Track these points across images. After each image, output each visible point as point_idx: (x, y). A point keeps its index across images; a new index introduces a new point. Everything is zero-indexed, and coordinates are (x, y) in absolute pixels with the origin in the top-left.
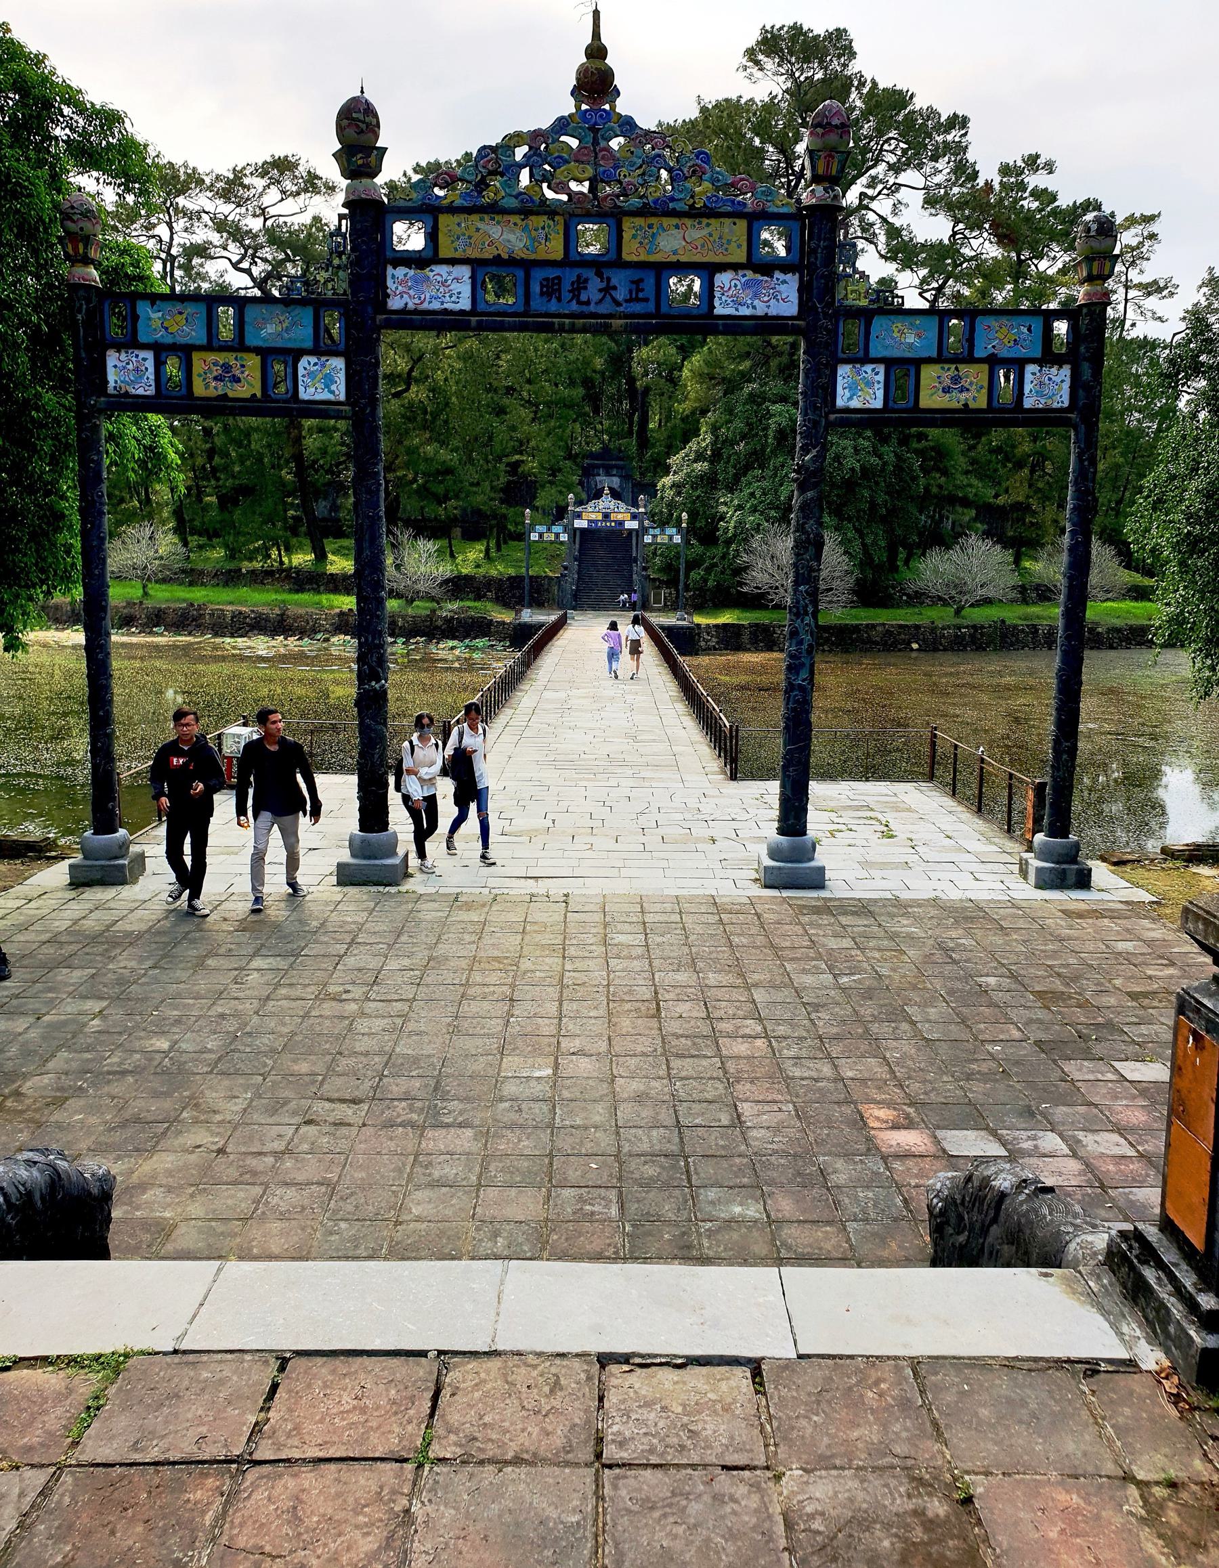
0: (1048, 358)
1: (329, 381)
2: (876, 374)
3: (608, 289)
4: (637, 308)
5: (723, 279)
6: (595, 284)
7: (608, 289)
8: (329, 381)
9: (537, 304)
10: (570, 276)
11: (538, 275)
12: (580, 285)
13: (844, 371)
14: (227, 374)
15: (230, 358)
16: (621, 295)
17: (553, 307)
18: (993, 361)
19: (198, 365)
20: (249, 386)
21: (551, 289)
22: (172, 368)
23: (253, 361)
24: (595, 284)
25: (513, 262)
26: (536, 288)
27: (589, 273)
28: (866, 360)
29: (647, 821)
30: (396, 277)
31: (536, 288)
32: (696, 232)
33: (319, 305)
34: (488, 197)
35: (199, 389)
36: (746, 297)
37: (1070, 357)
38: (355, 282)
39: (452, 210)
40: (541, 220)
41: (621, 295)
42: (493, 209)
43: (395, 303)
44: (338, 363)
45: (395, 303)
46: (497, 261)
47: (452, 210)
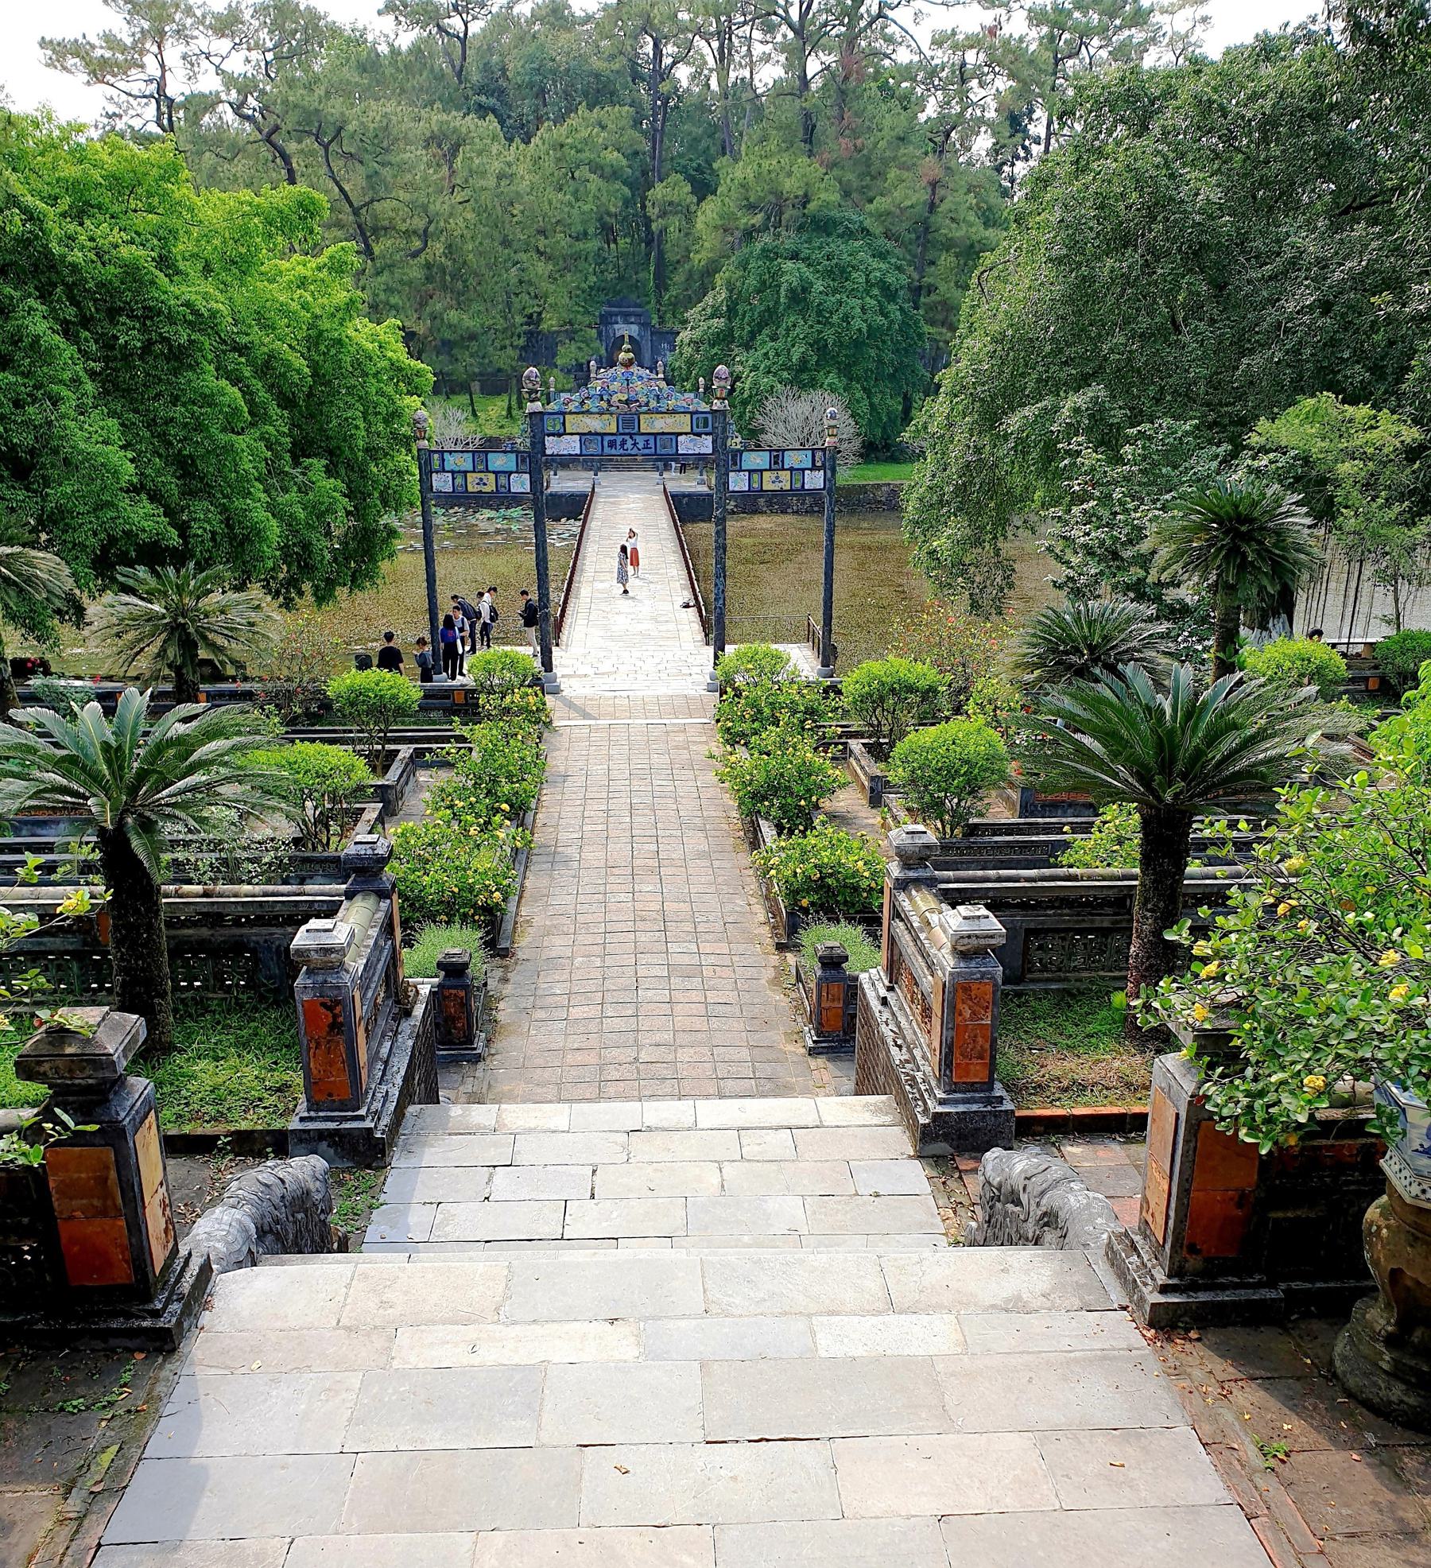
0: (814, 468)
1: (523, 484)
2: (745, 476)
3: (635, 444)
4: (647, 451)
5: (680, 438)
6: (630, 442)
7: (635, 444)
8: (523, 484)
9: (607, 450)
10: (619, 439)
11: (607, 439)
12: (624, 442)
13: (731, 474)
14: (481, 482)
15: (482, 475)
16: (640, 446)
17: (613, 452)
18: (791, 469)
19: (469, 480)
20: (490, 487)
21: (612, 444)
22: (459, 480)
23: (492, 477)
24: (630, 442)
25: (597, 434)
26: (606, 444)
27: (627, 437)
28: (740, 470)
29: (660, 667)
30: (549, 441)
31: (606, 444)
32: (670, 419)
33: (518, 452)
34: (586, 408)
35: (470, 489)
36: (691, 445)
37: (823, 467)
38: (533, 444)
39: (571, 413)
40: (606, 417)
41: (640, 446)
42: (588, 412)
43: (548, 452)
44: (527, 476)
45: (548, 452)
46: (590, 433)
47: (571, 413)
